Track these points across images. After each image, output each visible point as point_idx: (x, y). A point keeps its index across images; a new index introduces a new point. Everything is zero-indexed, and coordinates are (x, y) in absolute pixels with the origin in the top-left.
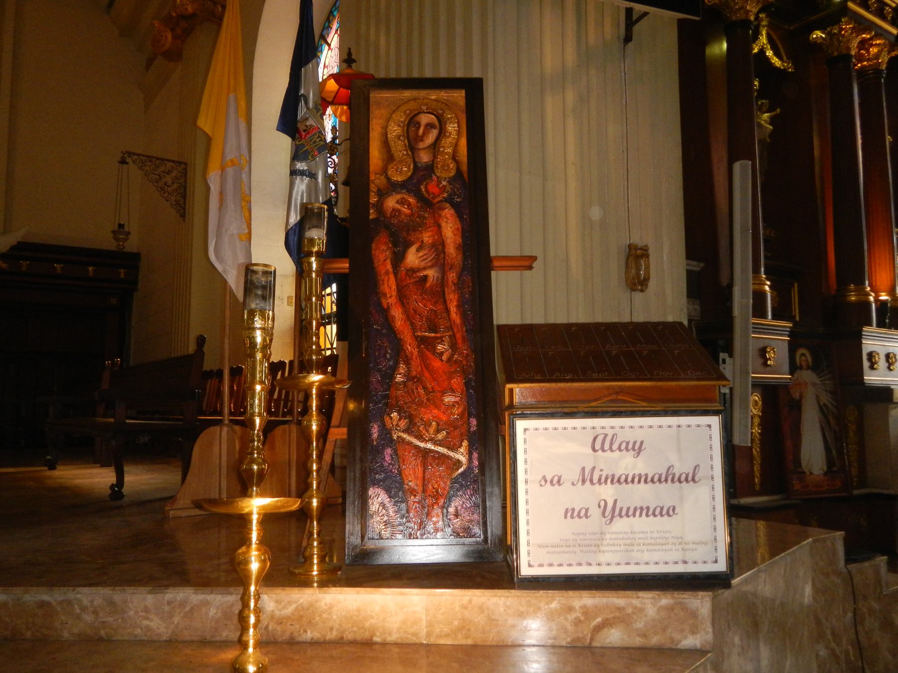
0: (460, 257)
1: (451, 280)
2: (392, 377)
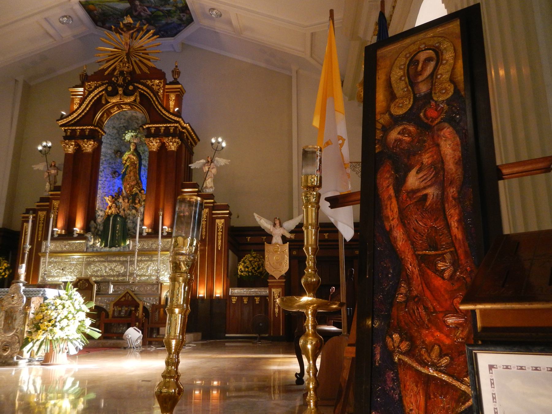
0: (460, 171)
1: (451, 195)
2: (394, 297)
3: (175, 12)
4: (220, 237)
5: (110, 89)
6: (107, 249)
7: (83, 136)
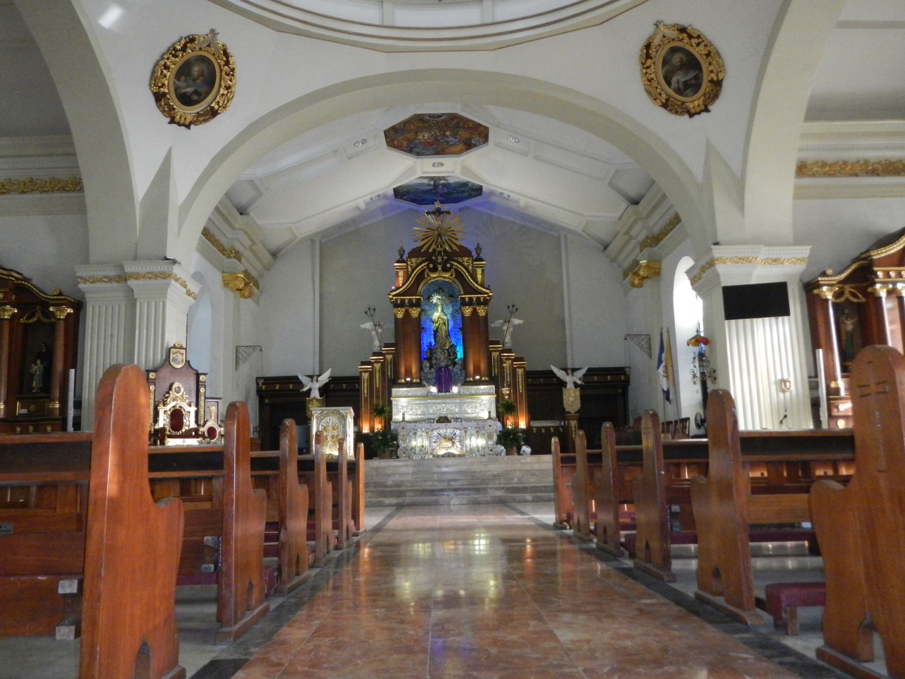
3: (468, 191)
4: (520, 383)
5: (431, 266)
6: (443, 394)
7: (412, 305)
